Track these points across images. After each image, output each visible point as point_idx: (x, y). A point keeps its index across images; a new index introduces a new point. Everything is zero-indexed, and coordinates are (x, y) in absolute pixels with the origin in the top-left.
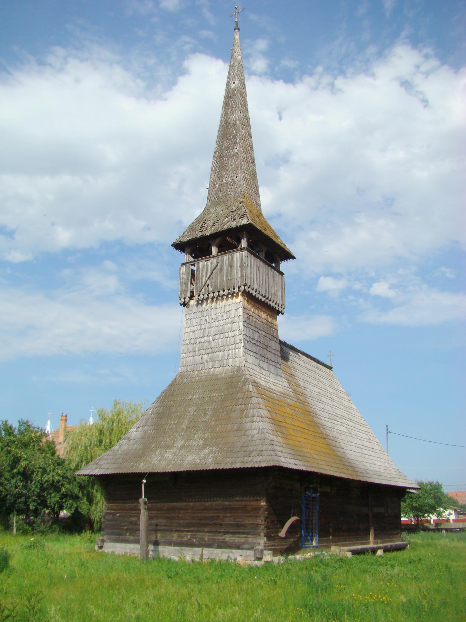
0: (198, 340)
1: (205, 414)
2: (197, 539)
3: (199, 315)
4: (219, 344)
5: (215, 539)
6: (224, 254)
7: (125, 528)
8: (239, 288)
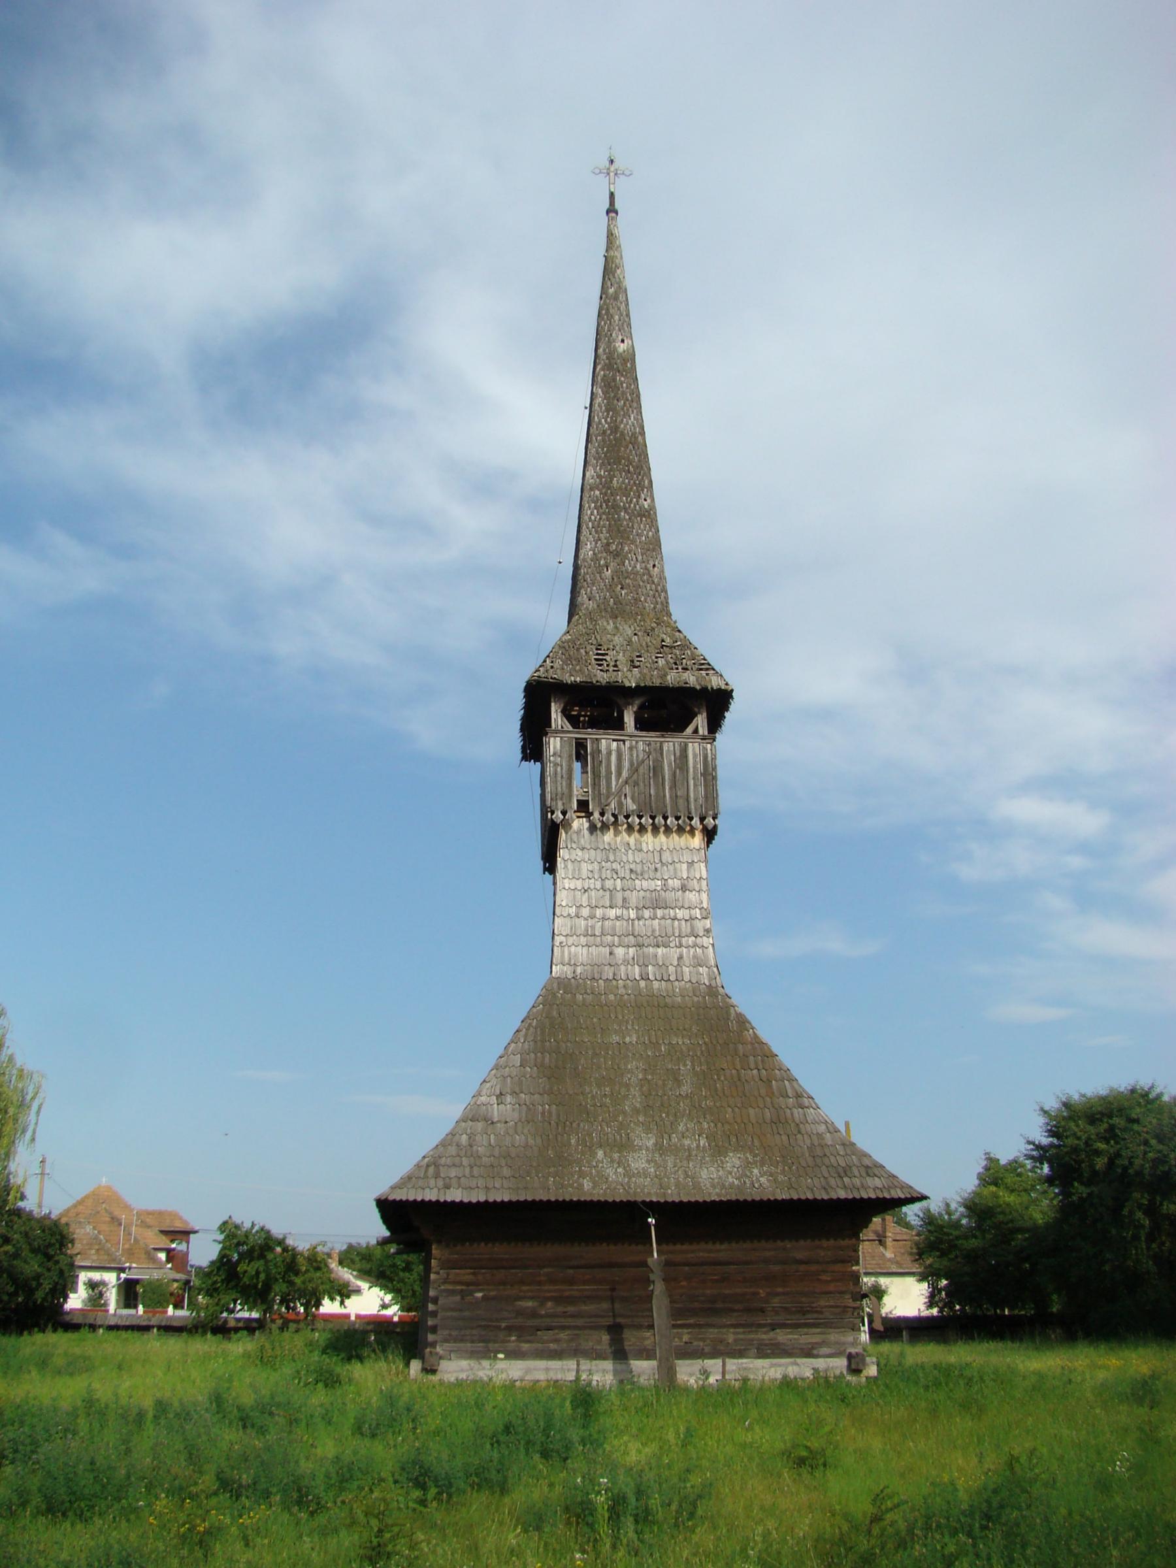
0: (599, 913)
1: (678, 1082)
2: (708, 1341)
3: (600, 855)
4: (653, 931)
5: (752, 1340)
6: (663, 736)
7: (503, 1325)
8: (702, 819)
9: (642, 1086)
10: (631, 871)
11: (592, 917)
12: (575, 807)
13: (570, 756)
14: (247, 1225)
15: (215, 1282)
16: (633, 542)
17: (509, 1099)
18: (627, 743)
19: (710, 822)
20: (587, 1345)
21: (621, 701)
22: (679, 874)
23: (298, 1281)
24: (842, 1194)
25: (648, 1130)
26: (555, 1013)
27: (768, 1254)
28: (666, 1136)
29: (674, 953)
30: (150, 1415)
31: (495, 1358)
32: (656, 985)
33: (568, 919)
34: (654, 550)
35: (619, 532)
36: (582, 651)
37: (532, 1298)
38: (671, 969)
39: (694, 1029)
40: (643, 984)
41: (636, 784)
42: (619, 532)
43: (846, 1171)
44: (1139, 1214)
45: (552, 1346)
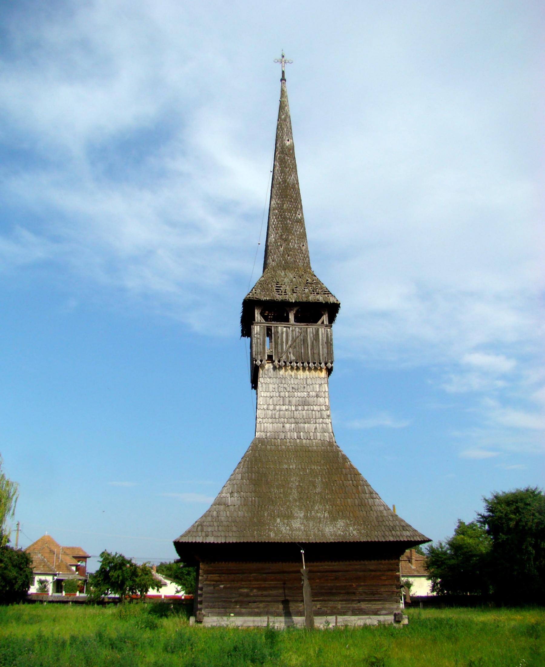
1: (315, 487)
3: (278, 381)
4: (303, 416)
5: (350, 607)
6: (307, 325)
7: (233, 600)
8: (326, 364)
9: (298, 489)
10: (293, 388)
11: (275, 409)
12: (266, 358)
13: (264, 334)
14: (114, 554)
15: (99, 581)
16: (293, 234)
17: (236, 494)
18: (291, 328)
19: (329, 365)
20: (273, 609)
21: (288, 309)
22: (315, 389)
23: (137, 580)
24: (391, 539)
25: (301, 509)
26: (257, 455)
27: (357, 567)
28: (309, 512)
29: (313, 426)
30: (68, 642)
31: (230, 616)
32: (304, 441)
33: (263, 411)
34: (303, 238)
35: (287, 229)
36: (270, 285)
37: (246, 588)
38: (312, 434)
39: (322, 462)
40: (298, 441)
41: (295, 347)
42: (287, 229)
43: (393, 528)
44: (530, 548)
45: (256, 610)
